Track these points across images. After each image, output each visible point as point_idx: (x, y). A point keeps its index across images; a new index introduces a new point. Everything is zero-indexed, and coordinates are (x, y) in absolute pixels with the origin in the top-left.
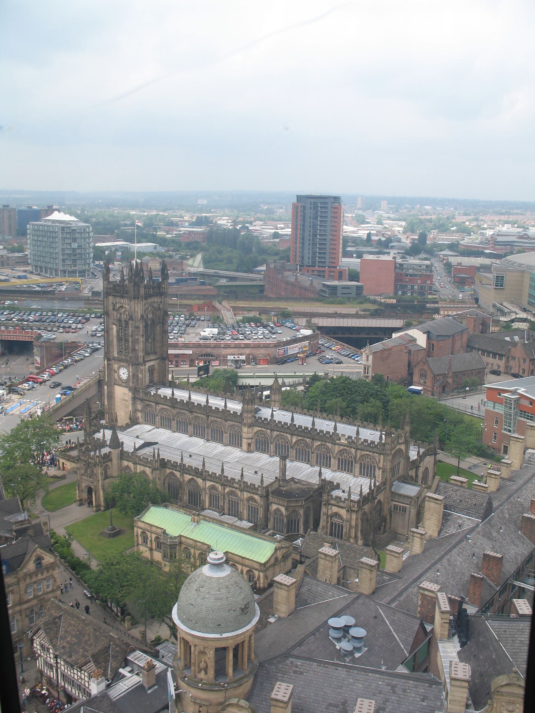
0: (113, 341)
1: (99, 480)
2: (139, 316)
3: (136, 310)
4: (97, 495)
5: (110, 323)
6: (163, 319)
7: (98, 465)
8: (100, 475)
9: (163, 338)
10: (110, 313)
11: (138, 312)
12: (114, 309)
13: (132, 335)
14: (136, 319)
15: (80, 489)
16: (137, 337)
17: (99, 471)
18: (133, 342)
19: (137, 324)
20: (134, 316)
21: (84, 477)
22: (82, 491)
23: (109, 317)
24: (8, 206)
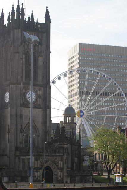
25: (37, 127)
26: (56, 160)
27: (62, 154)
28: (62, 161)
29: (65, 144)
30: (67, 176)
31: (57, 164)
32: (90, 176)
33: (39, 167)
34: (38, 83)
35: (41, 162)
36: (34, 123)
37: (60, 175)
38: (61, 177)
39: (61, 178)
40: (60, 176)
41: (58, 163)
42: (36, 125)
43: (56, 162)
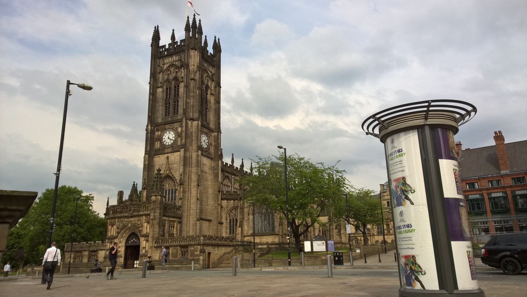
25: (175, 177)
26: (139, 223)
27: (149, 212)
28: (148, 223)
29: (153, 196)
30: (155, 247)
31: (140, 229)
32: (195, 246)
33: (114, 235)
34: (179, 117)
35: (118, 228)
36: (172, 173)
37: (144, 246)
38: (145, 249)
39: (146, 251)
40: (144, 248)
41: (142, 226)
42: (173, 175)
43: (139, 225)
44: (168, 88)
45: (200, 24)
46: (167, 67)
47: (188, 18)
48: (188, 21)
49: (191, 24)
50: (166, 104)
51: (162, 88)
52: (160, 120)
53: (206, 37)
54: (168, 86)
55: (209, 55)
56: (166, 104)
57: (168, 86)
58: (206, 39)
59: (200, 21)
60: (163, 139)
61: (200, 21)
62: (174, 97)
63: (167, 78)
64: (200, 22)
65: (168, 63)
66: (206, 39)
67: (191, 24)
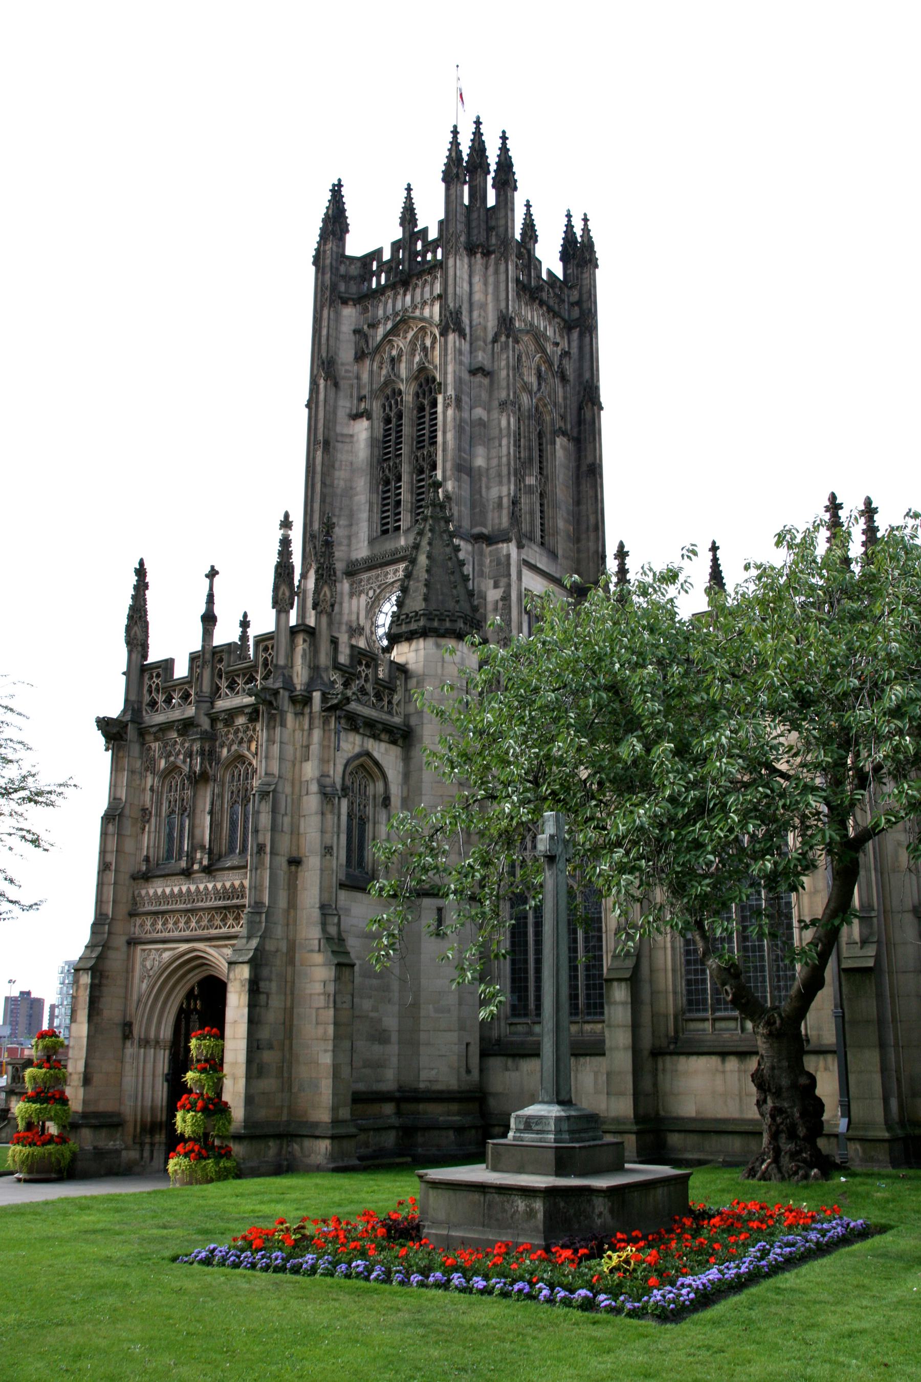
0: (349, 491)
1: (295, 862)
2: (491, 324)
3: (478, 297)
4: (272, 1015)
5: (342, 414)
6: (580, 422)
7: (303, 701)
8: (312, 802)
9: (578, 502)
10: (342, 371)
11: (483, 306)
12: (360, 356)
13: (458, 400)
14: (480, 333)
15: (111, 1010)
16: (479, 412)
17: (310, 770)
18: (460, 429)
19: (480, 356)
20: (465, 319)
21: (159, 888)
22: (127, 1030)
23: (336, 385)
24: (29, 993)
44: (392, 414)
45: (504, 149)
46: (386, 335)
47: (455, 132)
48: (455, 143)
49: (466, 158)
50: (387, 482)
51: (368, 419)
52: (361, 551)
53: (528, 206)
54: (391, 410)
55: (544, 276)
56: (387, 482)
57: (391, 410)
58: (528, 215)
59: (504, 138)
60: (378, 627)
61: (504, 138)
62: (418, 448)
63: (388, 376)
64: (504, 144)
65: (387, 318)
66: (528, 215)
67: (466, 158)
